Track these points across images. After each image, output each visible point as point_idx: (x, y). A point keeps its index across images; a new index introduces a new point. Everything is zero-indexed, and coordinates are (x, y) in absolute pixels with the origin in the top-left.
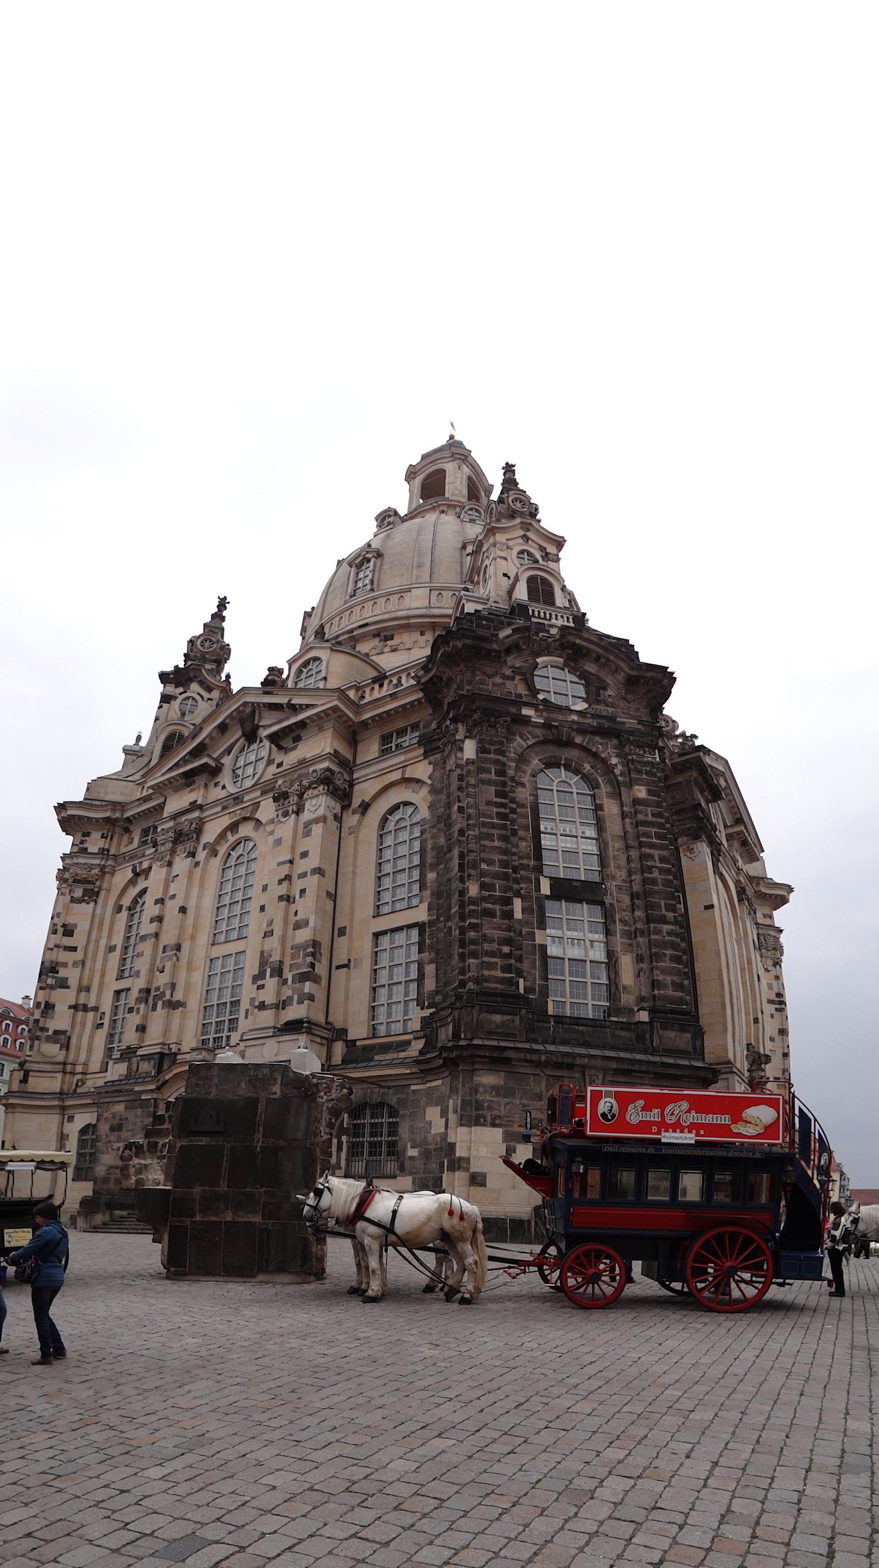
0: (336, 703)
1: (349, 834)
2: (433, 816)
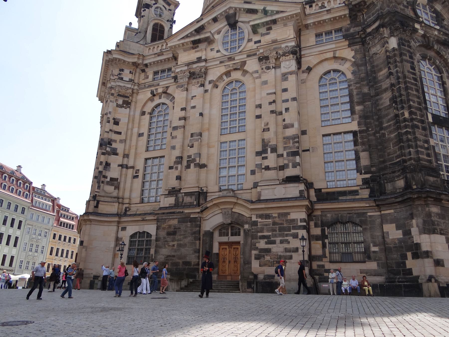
0: (299, 11)
1: (301, 83)
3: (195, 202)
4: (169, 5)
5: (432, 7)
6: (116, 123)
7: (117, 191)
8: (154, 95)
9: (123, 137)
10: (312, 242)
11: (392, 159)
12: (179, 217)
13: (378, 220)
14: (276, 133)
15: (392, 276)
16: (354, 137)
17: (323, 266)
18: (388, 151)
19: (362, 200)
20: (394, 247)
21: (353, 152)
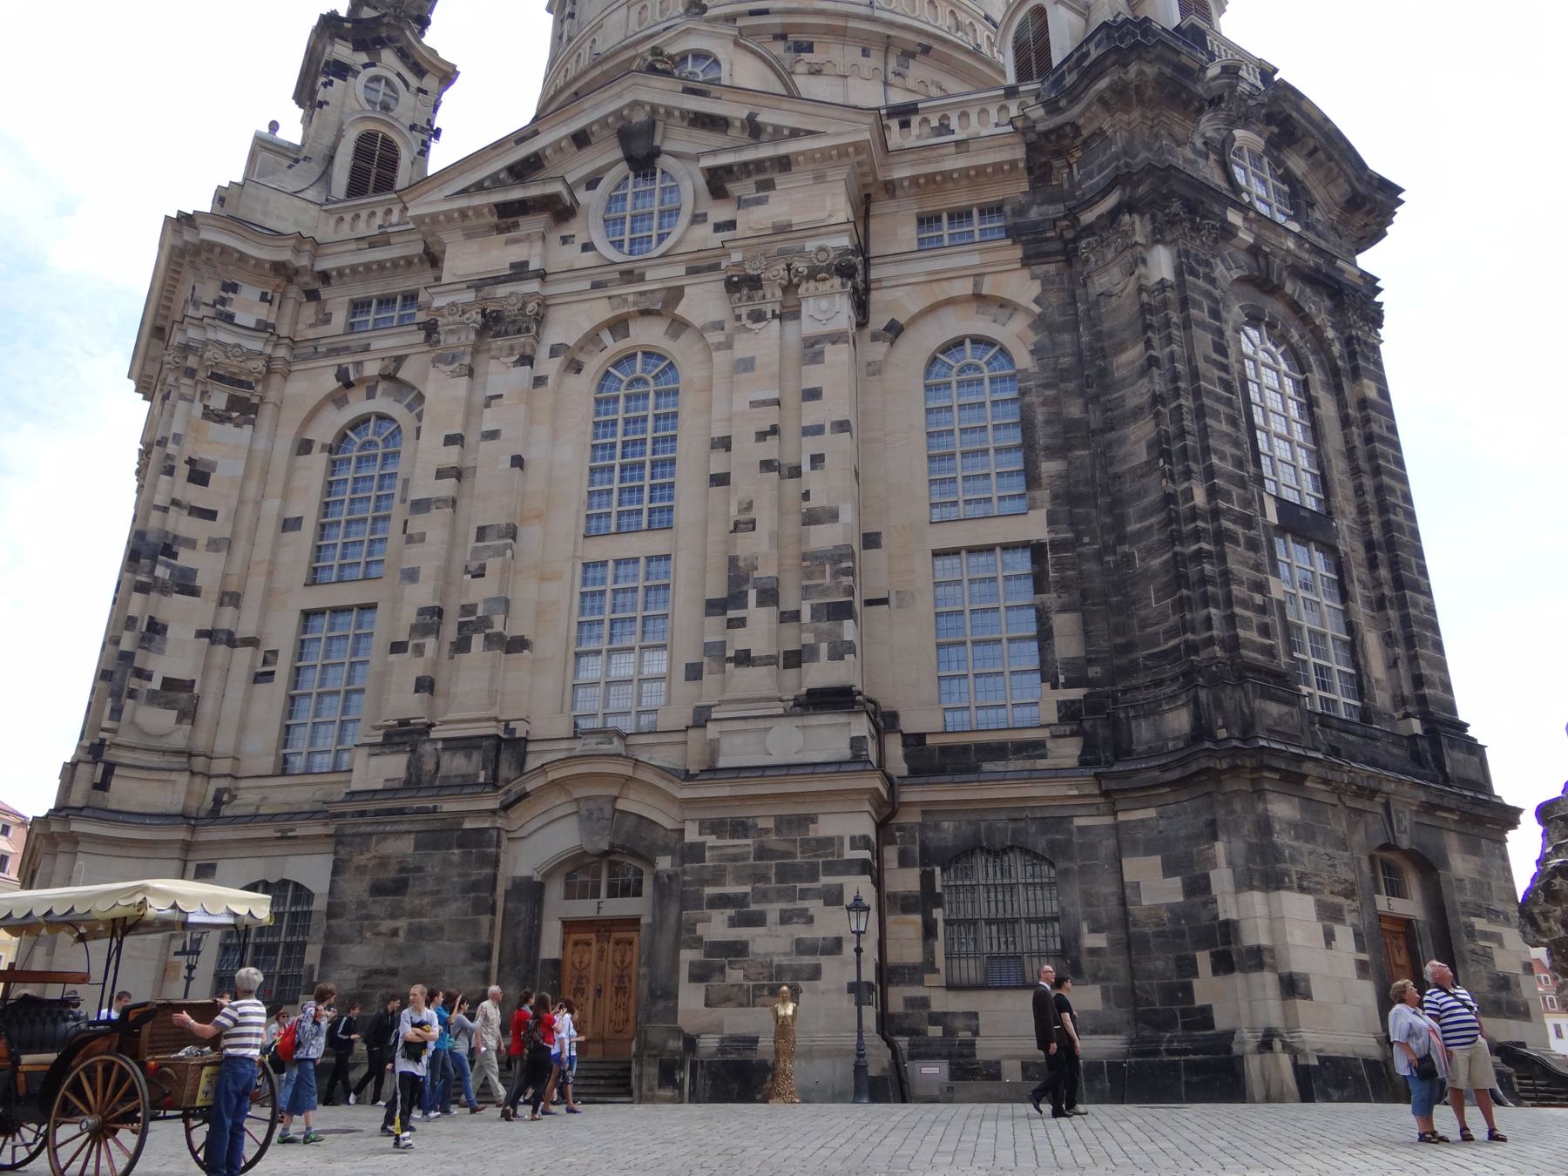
0: (866, 136)
2: (1043, 368)
3: (482, 774)
4: (420, 72)
5: (1277, 163)
6: (199, 476)
7: (186, 727)
8: (349, 385)
9: (220, 528)
10: (889, 919)
11: (1152, 641)
12: (417, 827)
13: (1105, 843)
14: (777, 539)
15: (1147, 1033)
16: (1034, 562)
17: (924, 1002)
18: (1143, 613)
19: (1057, 773)
20: (1156, 935)
21: (1032, 612)
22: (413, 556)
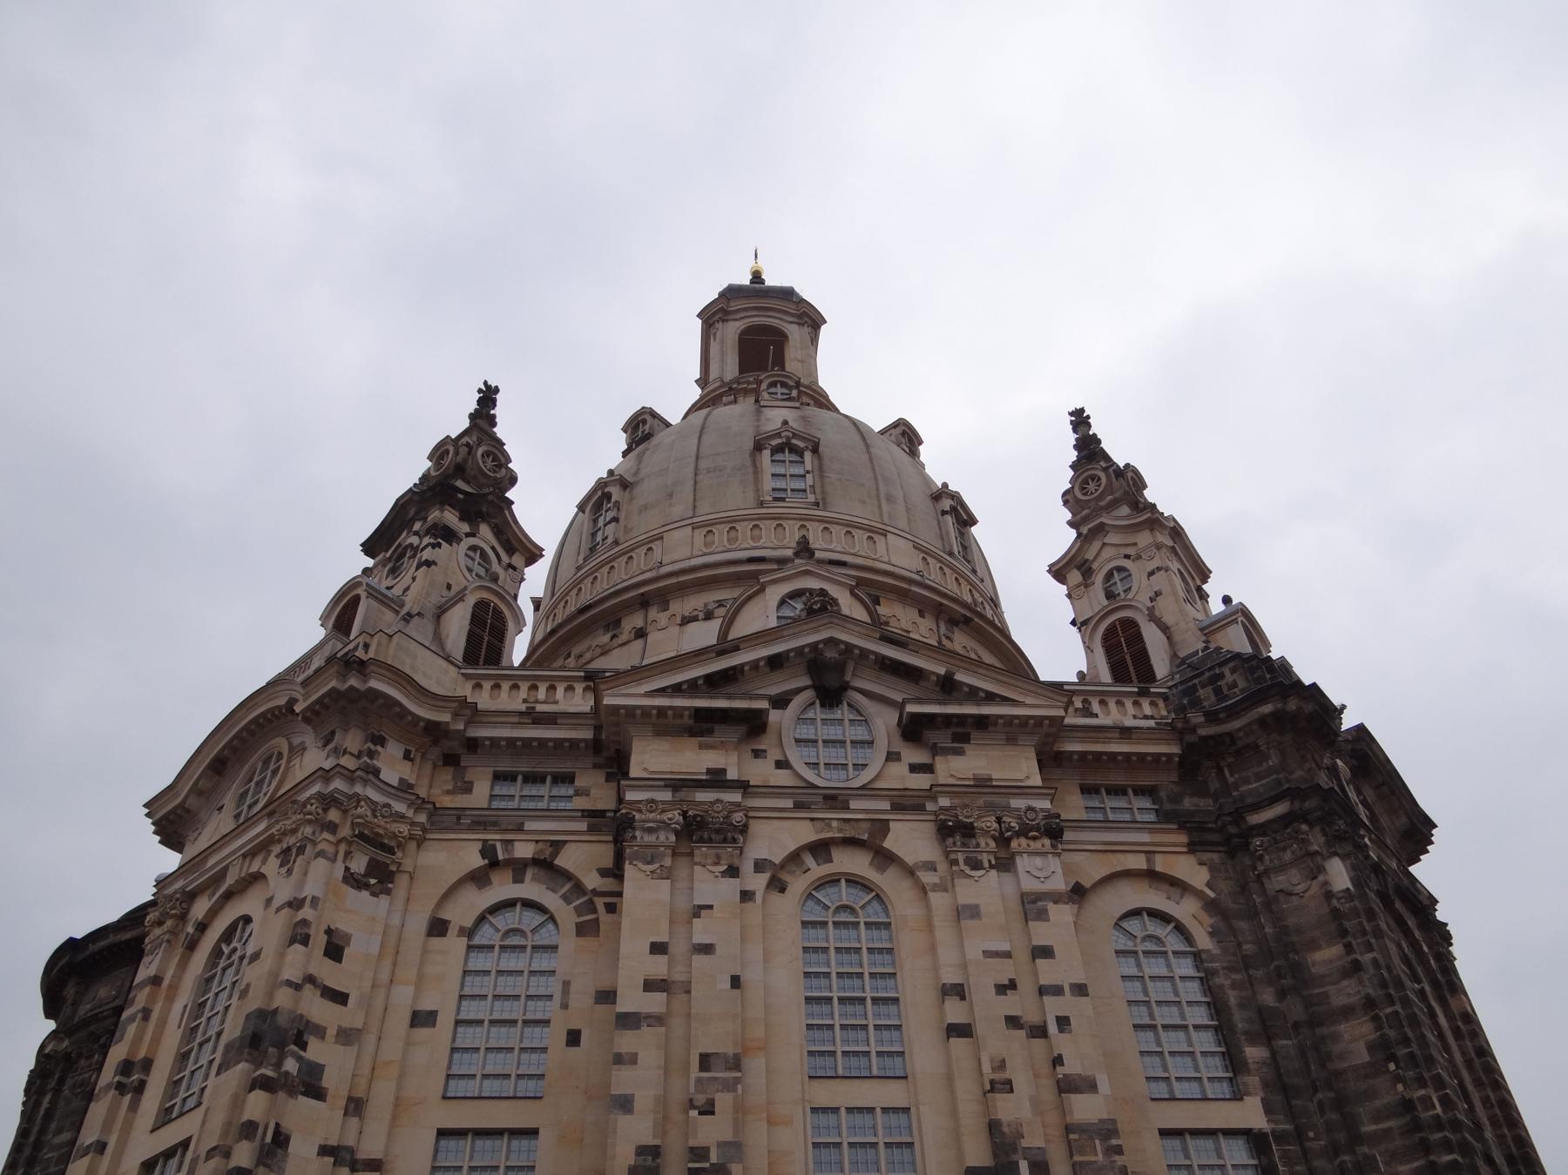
4: (511, 551)
5: (1359, 792)
6: (335, 951)
8: (494, 864)
14: (1035, 1103)
22: (624, 1081)
